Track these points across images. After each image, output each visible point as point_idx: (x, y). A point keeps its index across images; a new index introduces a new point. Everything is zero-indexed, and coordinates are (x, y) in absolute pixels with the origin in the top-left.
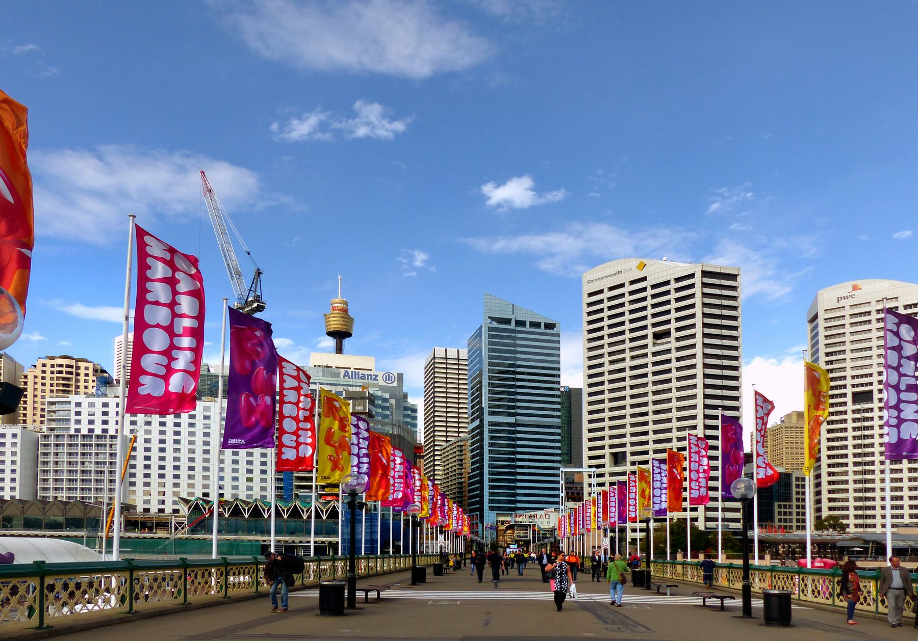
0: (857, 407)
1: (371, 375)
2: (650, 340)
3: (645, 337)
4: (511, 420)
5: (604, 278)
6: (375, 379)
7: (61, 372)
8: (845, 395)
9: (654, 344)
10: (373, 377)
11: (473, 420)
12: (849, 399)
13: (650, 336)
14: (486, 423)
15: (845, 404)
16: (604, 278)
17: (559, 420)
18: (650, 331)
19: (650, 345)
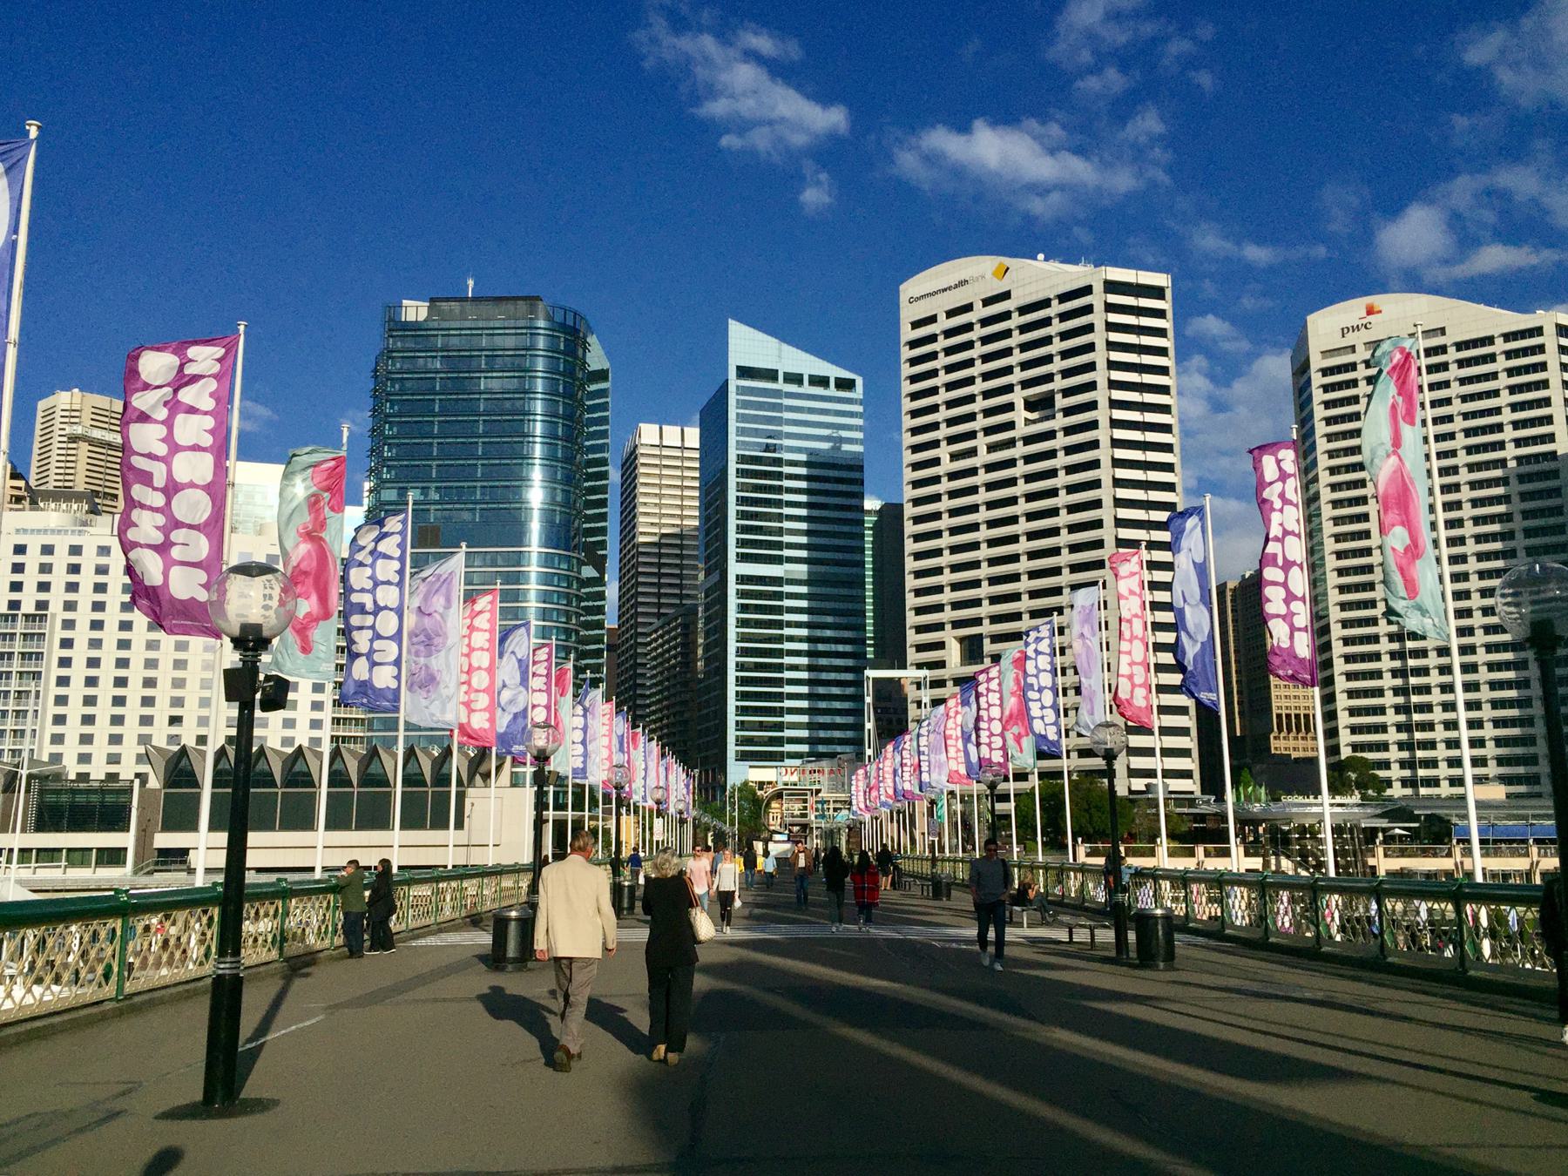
5: (936, 293)
14: (731, 579)
16: (936, 293)
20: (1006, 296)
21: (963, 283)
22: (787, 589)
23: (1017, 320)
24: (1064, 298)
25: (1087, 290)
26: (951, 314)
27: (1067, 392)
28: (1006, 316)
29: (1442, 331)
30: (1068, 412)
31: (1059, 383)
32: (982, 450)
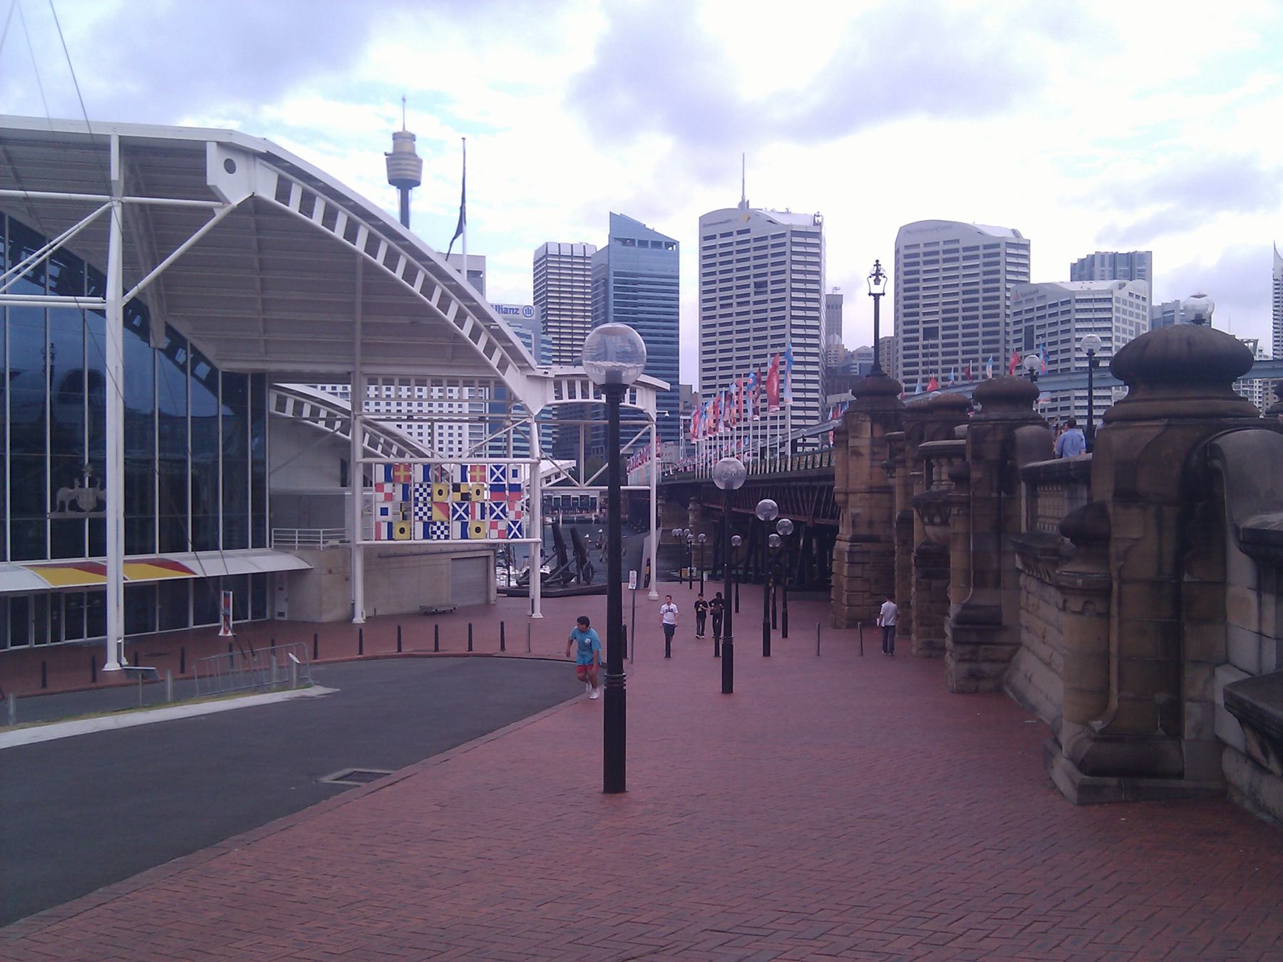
0: (925, 342)
1: (512, 309)
2: (751, 290)
6: (516, 313)
8: (917, 331)
9: (756, 293)
10: (515, 311)
12: (920, 335)
13: (752, 285)
15: (917, 339)
18: (751, 281)
19: (752, 294)
20: (747, 231)
24: (774, 237)
25: (783, 235)
26: (723, 236)
27: (773, 283)
28: (747, 241)
29: (957, 241)
30: (773, 292)
31: (770, 278)
32: (735, 304)
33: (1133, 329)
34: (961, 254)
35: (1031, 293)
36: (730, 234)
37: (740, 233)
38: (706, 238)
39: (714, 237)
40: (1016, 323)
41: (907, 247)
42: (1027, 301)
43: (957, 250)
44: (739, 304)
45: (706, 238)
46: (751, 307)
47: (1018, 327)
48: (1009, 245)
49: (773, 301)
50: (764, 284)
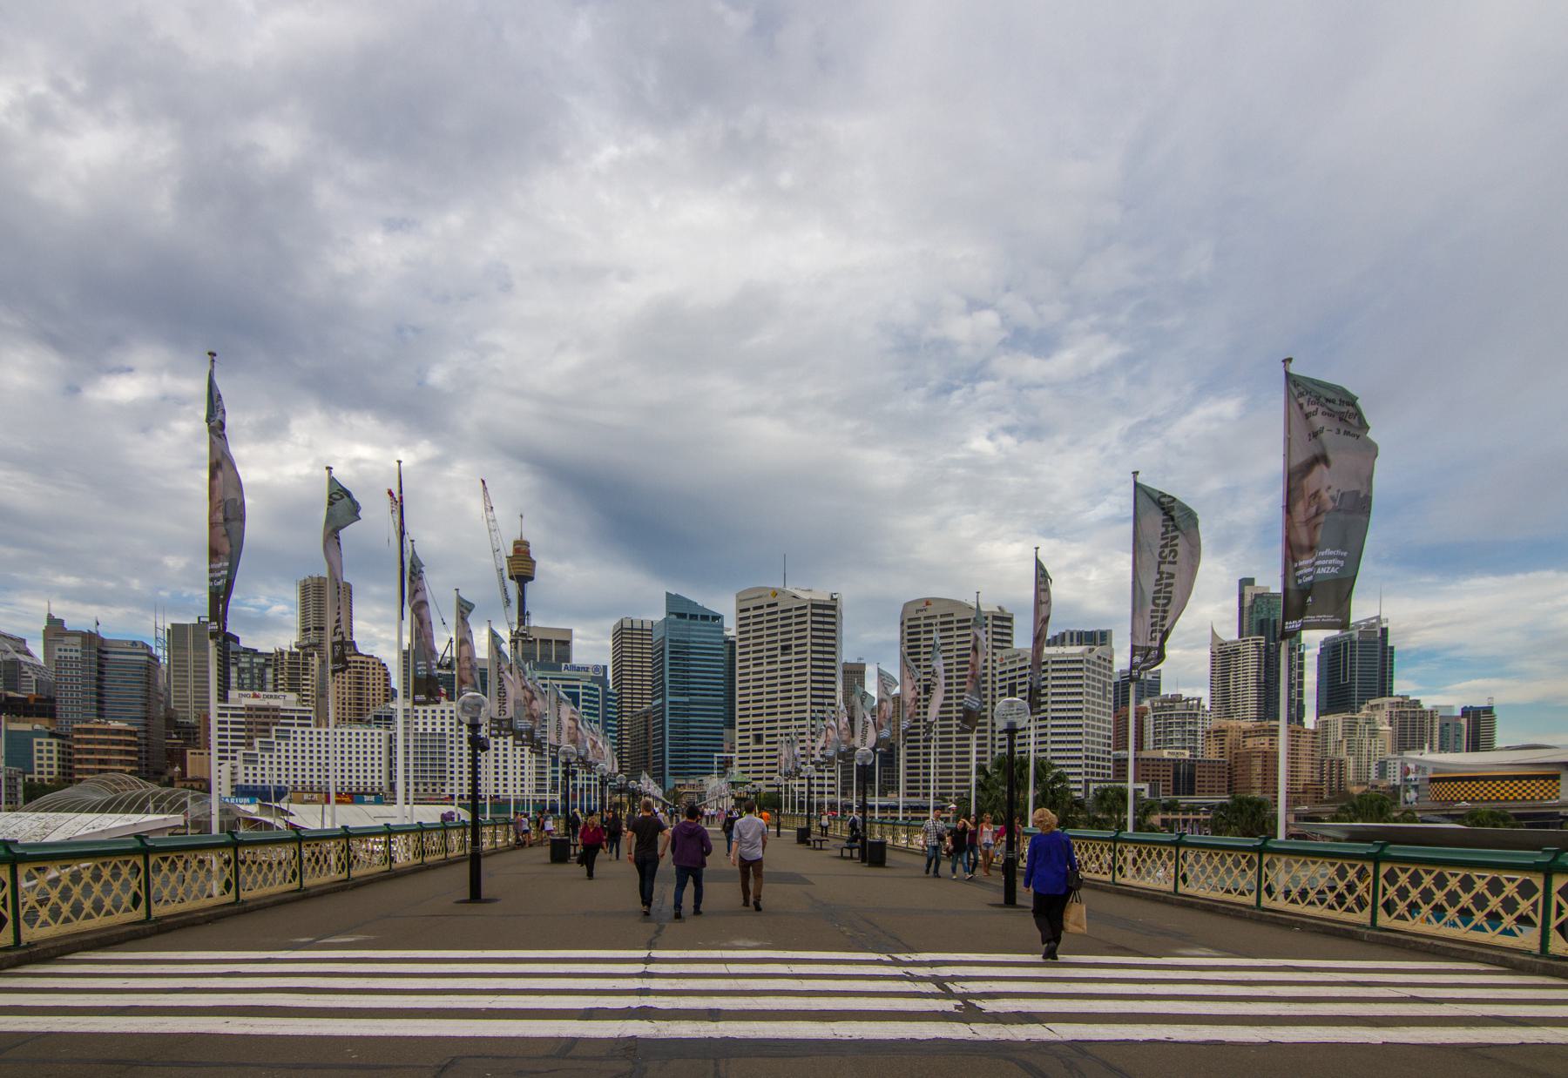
2: (779, 652)
3: (776, 649)
4: (686, 699)
7: (356, 667)
9: (782, 654)
11: (658, 697)
14: (667, 702)
17: (722, 699)
18: (779, 644)
20: (776, 605)
21: (759, 597)
22: (691, 706)
23: (780, 615)
24: (797, 609)
25: (805, 607)
26: (755, 608)
27: (796, 646)
28: (776, 613)
29: (952, 615)
30: (796, 653)
33: (1101, 686)
34: (955, 625)
35: (1015, 656)
36: (762, 607)
37: (769, 606)
38: (742, 611)
39: (748, 610)
40: (1001, 680)
41: (910, 620)
42: (1011, 663)
43: (952, 622)
44: (769, 663)
45: (742, 611)
46: (779, 666)
47: (1003, 684)
48: (995, 618)
49: (796, 660)
50: (789, 647)
